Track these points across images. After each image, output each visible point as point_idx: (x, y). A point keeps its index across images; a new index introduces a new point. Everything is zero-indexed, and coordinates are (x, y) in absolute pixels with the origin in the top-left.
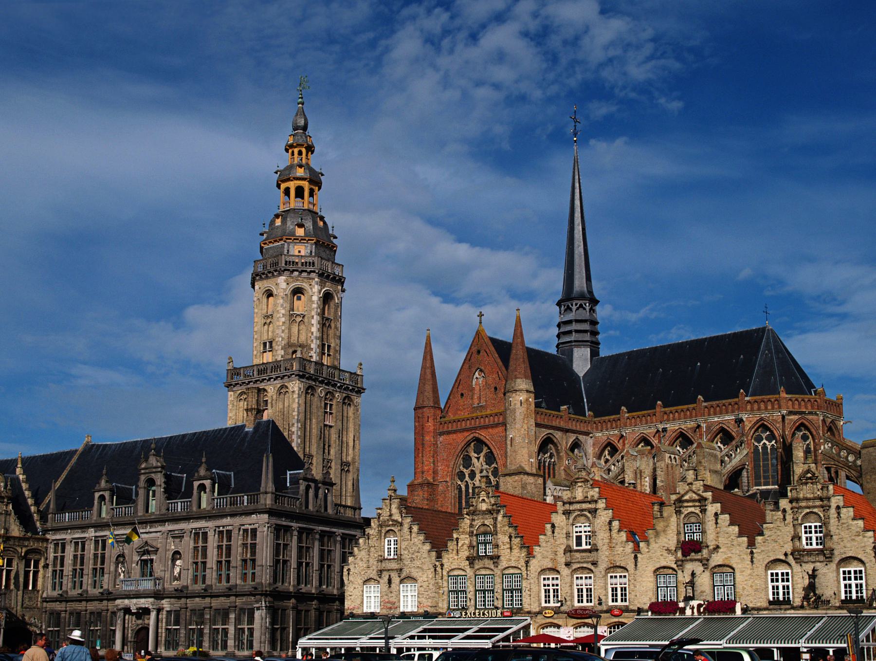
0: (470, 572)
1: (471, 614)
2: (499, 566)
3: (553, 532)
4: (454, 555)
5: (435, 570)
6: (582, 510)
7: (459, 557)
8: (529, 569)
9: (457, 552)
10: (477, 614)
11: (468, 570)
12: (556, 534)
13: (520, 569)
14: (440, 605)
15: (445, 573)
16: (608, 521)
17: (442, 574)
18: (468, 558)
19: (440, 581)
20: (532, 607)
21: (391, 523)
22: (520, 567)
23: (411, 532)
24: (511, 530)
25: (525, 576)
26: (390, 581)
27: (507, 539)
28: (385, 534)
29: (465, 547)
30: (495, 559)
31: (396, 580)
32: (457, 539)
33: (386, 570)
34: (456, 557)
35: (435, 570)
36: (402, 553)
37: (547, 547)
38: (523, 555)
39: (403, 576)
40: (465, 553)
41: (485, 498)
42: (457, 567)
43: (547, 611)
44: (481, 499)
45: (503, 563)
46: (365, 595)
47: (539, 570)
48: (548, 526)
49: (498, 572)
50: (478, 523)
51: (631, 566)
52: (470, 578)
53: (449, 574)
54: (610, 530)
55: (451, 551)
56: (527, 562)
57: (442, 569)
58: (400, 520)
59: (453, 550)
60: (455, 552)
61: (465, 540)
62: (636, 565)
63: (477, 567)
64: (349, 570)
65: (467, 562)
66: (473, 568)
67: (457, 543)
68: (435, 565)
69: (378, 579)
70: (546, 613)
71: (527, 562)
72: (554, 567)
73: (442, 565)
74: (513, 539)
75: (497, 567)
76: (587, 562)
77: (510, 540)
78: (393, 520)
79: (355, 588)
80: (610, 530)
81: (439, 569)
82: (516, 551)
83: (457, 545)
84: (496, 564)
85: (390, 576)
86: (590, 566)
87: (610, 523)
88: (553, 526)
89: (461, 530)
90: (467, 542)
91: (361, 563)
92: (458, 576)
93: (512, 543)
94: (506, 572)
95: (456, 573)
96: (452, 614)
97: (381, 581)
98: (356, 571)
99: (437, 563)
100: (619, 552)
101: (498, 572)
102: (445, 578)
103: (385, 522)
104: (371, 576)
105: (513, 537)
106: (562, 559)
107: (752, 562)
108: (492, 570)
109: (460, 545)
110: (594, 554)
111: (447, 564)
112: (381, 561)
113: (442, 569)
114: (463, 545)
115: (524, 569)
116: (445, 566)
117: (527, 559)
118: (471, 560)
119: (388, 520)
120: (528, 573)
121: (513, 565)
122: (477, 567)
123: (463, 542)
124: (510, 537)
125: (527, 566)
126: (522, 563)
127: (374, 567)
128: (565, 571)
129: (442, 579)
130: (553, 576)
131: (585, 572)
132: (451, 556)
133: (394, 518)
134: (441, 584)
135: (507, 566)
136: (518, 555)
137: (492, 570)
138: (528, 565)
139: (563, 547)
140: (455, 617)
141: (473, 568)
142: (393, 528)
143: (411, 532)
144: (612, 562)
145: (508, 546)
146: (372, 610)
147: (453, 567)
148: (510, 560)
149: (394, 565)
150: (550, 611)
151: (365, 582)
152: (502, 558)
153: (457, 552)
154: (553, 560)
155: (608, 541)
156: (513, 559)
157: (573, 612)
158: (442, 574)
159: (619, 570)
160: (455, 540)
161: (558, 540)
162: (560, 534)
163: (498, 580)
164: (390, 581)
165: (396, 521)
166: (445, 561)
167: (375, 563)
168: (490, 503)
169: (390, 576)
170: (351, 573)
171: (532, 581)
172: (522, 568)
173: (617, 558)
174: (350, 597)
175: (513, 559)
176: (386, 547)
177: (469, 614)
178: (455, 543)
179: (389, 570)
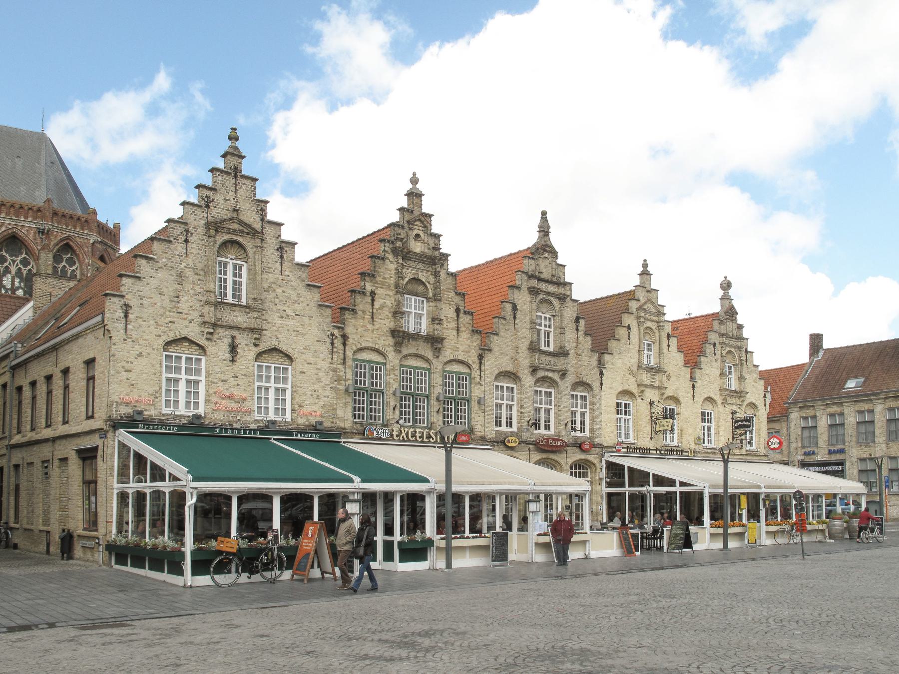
0: (393, 359)
1: (407, 436)
2: (441, 358)
3: (515, 318)
4: (366, 321)
5: (332, 344)
6: (549, 294)
7: (377, 327)
8: (483, 368)
9: (372, 318)
10: (418, 435)
11: (392, 355)
12: (517, 321)
13: (469, 366)
14: (340, 413)
15: (349, 354)
16: (575, 317)
17: (344, 354)
18: (394, 333)
19: (341, 367)
20: (486, 429)
21: (236, 226)
22: (471, 363)
23: (281, 257)
24: (457, 299)
25: (477, 379)
26: (233, 349)
27: (452, 313)
28: (220, 246)
29: (386, 312)
30: (435, 342)
31: (247, 353)
32: (373, 294)
33: (222, 326)
34: (370, 327)
35: (332, 344)
36: (263, 298)
37: (506, 338)
38: (475, 344)
39: (263, 346)
40: (385, 323)
41: (421, 233)
42: (370, 345)
43: (510, 438)
44: (415, 232)
45: (447, 354)
46: (165, 375)
47: (497, 372)
48: (509, 307)
49: (440, 368)
50: (409, 274)
51: (596, 385)
52: (394, 369)
53: (355, 357)
54: (577, 330)
55: (360, 313)
56: (481, 357)
57: (344, 344)
58: (257, 226)
59: (364, 312)
60: (368, 317)
61: (386, 298)
62: (601, 384)
63: (405, 351)
64: (127, 308)
65: (391, 341)
66: (400, 352)
67: (373, 300)
68: (332, 335)
69: (203, 342)
70: (509, 442)
71: (481, 357)
72: (515, 372)
73: (345, 337)
74: (461, 315)
75: (438, 357)
76: (553, 371)
77: (458, 316)
78: (241, 222)
79: (140, 355)
80: (577, 330)
81: (338, 343)
82: (465, 335)
83: (373, 305)
84: (437, 351)
85: (233, 338)
86: (556, 376)
87: (577, 320)
88: (515, 308)
89: (379, 279)
90: (390, 302)
91: (157, 299)
92: (369, 362)
93: (461, 320)
94: (449, 368)
95: (365, 356)
96: (375, 433)
97: (211, 348)
98: (145, 316)
99: (336, 332)
100: (585, 363)
101: (437, 365)
102: (349, 362)
103: (224, 220)
104: (185, 333)
105: (462, 311)
106: (525, 360)
107: (694, 397)
108: (427, 360)
109: (377, 305)
110: (562, 360)
111: (354, 336)
112: (215, 305)
113: (344, 344)
114: (382, 307)
115: (475, 366)
116: (350, 341)
117: (480, 352)
118: (400, 337)
119: (231, 219)
120: (482, 375)
121: (460, 358)
122: (405, 351)
123: (383, 301)
124: (458, 311)
125: (480, 363)
126: (473, 359)
127: (195, 315)
128: (528, 380)
129: (344, 363)
130: (508, 385)
131: (545, 385)
132: (361, 322)
133: (242, 217)
134: (342, 373)
135: (452, 357)
136: (468, 342)
137: (427, 360)
138: (483, 361)
139: (526, 343)
140: (380, 439)
141: (400, 352)
142: (240, 239)
143: (281, 257)
144: (579, 375)
145: (453, 325)
146: (201, 411)
147: (363, 345)
148: (457, 349)
149: (240, 318)
150: (514, 439)
151: (168, 344)
152: (446, 342)
153: (372, 318)
154: (514, 360)
155: (574, 345)
156: (461, 348)
157: (544, 443)
158: (344, 354)
159: (580, 388)
160: (368, 294)
161: (520, 330)
162: (523, 320)
163: (438, 379)
164: (233, 349)
165: (249, 226)
166: (349, 330)
167: (197, 305)
168: (428, 245)
169: (233, 338)
170: (131, 317)
171: (487, 389)
172: (474, 366)
173: (583, 372)
174: (130, 375)
175: (461, 348)
176: (244, 280)
177: (404, 434)
178: (369, 300)
179: (231, 327)
